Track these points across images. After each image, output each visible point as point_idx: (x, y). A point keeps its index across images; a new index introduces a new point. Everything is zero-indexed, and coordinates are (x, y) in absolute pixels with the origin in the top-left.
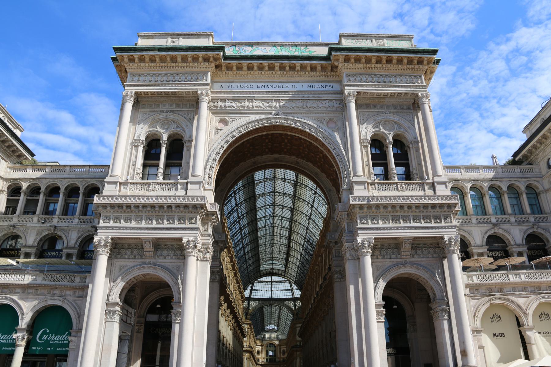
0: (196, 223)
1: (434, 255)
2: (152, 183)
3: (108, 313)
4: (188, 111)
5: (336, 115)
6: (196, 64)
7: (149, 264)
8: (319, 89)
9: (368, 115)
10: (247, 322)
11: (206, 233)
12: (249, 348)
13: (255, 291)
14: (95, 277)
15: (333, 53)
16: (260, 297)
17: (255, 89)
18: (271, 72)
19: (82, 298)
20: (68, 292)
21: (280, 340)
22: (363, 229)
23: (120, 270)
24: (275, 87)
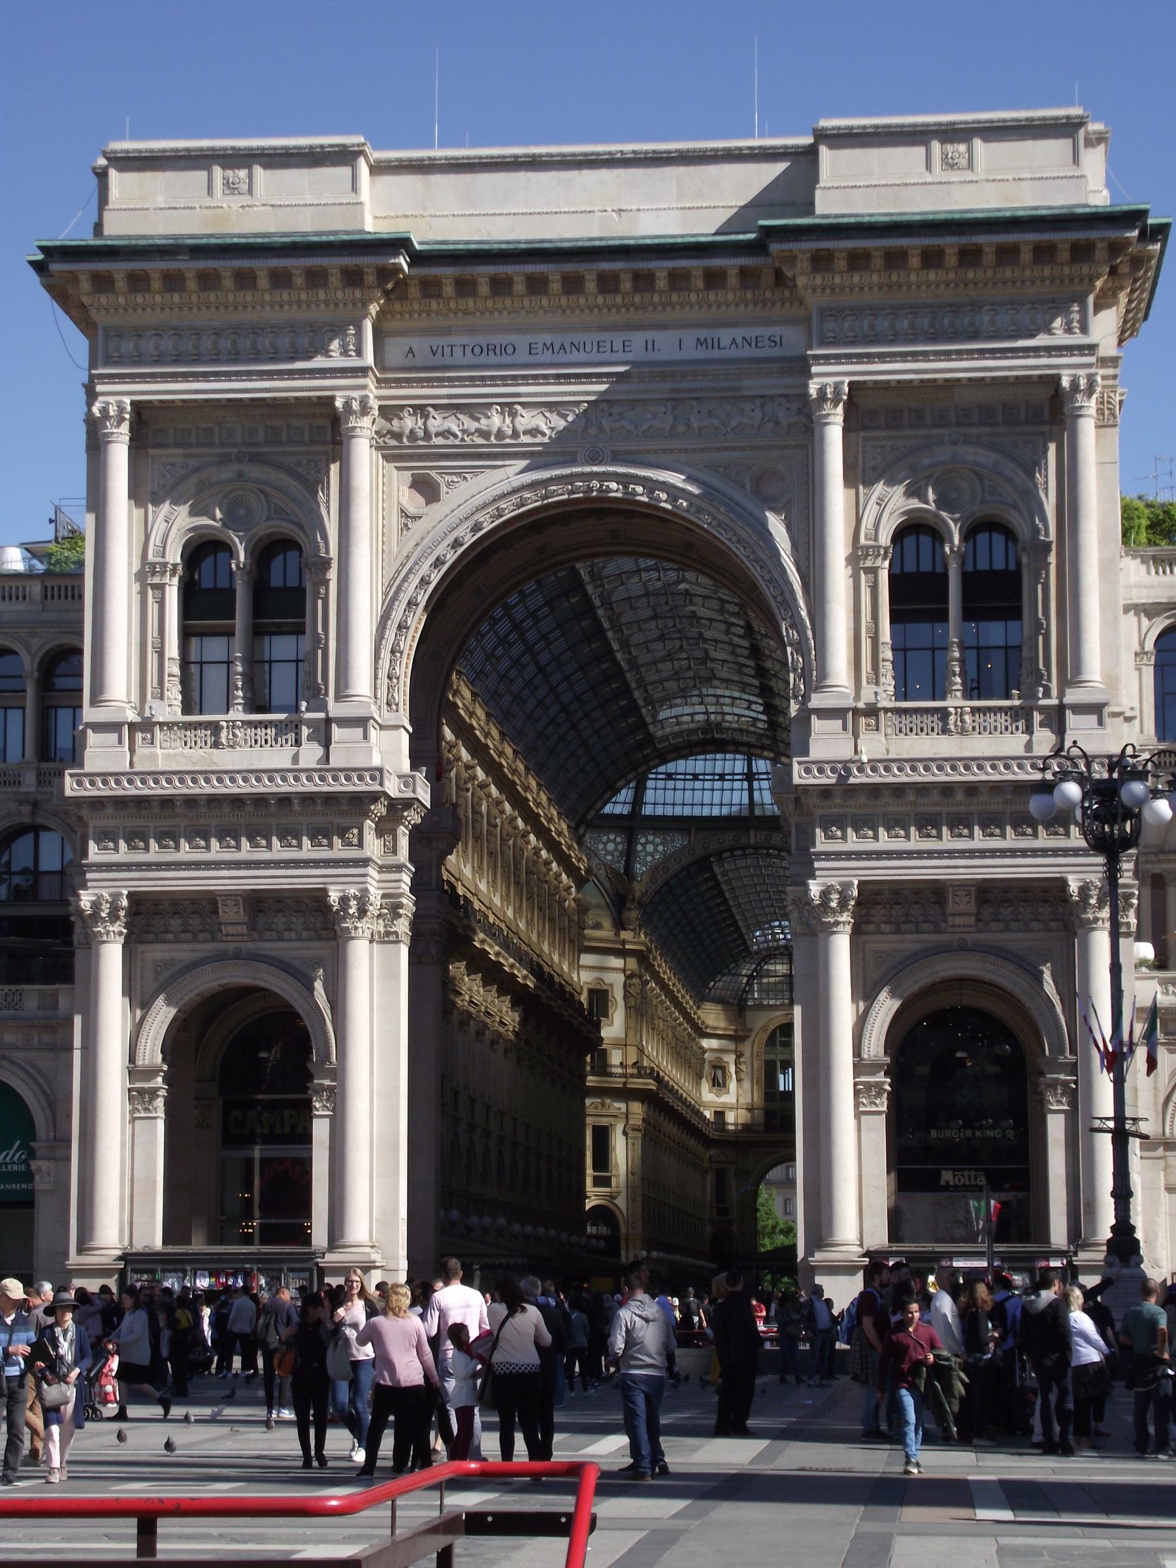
0: (360, 845)
1: (1053, 925)
2: (225, 724)
3: (138, 1097)
4: (308, 453)
6: (322, 295)
8: (733, 353)
10: (623, 942)
11: (391, 860)
12: (639, 1076)
13: (661, 784)
16: (687, 811)
18: (571, 298)
22: (828, 856)
23: (157, 974)
24: (588, 348)
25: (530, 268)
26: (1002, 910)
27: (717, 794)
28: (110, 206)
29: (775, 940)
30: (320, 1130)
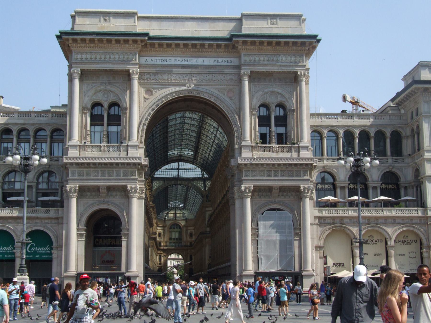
1: (295, 197)
3: (79, 235)
5: (234, 87)
6: (127, 46)
7: (104, 201)
8: (222, 64)
9: (259, 87)
14: (70, 213)
15: (234, 39)
16: (164, 176)
17: (173, 63)
19: (57, 225)
20: (46, 221)
21: (186, 220)
22: (246, 180)
24: (188, 61)
25: (176, 42)
26: (284, 193)
27: (171, 173)
28: (76, 24)
29: (172, 206)
30: (124, 244)
